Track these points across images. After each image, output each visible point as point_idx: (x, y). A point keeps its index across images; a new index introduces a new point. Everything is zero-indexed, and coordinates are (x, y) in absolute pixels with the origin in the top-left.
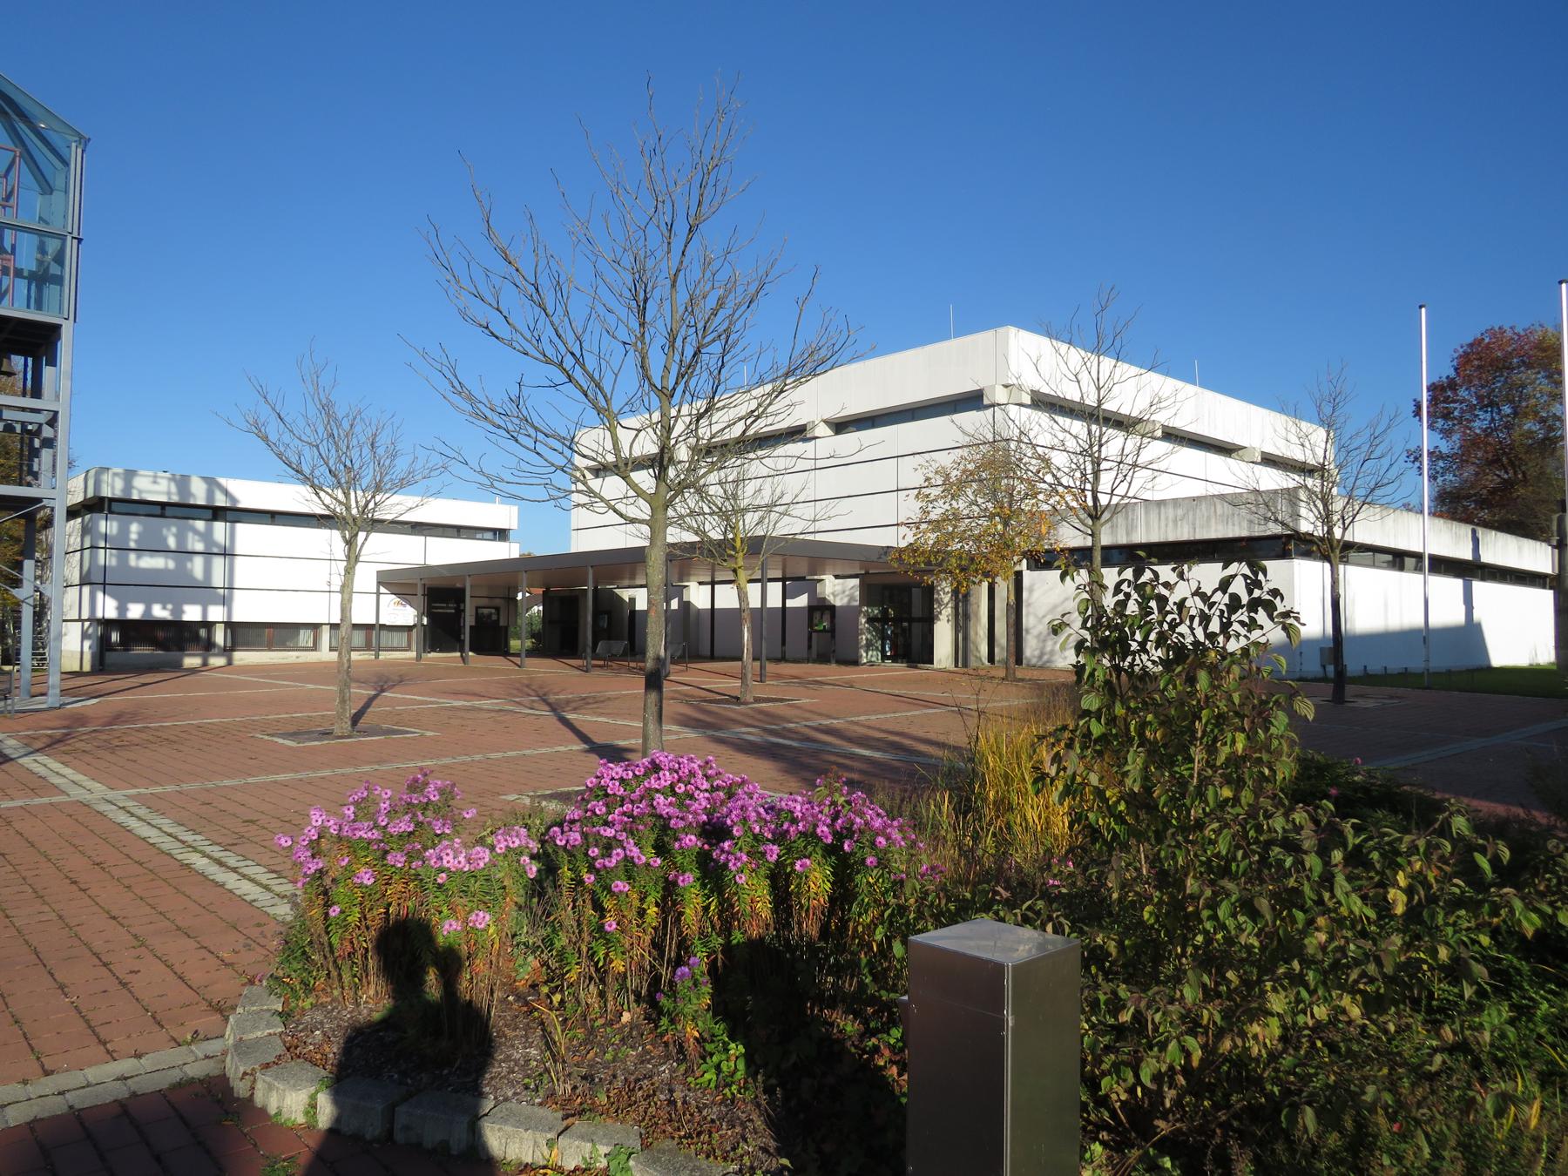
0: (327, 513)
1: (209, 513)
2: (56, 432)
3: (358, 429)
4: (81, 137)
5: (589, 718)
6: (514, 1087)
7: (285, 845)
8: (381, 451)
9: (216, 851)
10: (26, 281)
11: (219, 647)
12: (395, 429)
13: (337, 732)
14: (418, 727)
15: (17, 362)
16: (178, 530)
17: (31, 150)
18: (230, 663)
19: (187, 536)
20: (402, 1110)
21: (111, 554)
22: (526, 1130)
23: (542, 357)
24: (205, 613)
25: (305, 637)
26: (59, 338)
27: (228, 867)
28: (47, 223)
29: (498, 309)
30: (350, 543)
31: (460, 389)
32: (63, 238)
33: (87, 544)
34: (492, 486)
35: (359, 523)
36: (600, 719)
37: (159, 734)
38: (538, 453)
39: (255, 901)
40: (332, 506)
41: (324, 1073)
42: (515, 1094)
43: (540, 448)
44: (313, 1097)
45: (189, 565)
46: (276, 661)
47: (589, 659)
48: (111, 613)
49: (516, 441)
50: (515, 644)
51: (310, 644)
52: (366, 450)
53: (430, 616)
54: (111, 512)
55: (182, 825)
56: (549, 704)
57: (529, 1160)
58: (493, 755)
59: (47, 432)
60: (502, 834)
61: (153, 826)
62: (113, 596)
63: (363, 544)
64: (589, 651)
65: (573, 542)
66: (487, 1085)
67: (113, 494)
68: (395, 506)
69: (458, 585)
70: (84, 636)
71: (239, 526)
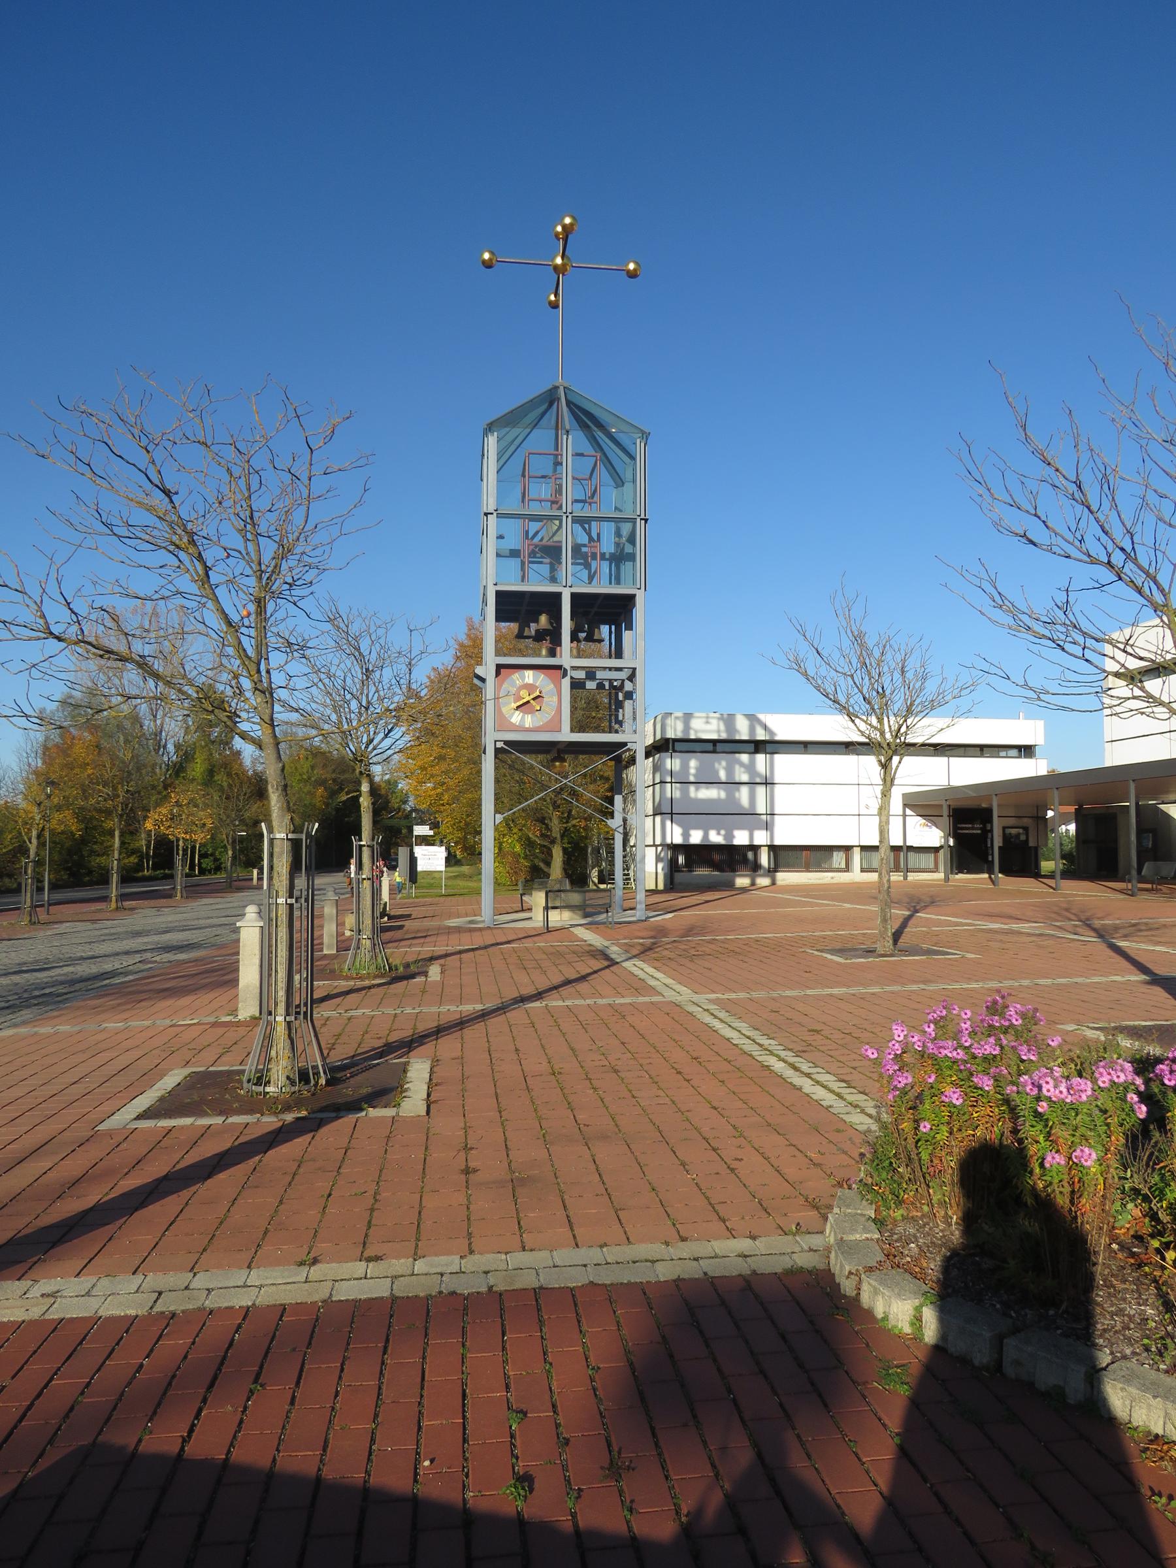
0: (863, 740)
1: (751, 747)
2: (635, 685)
3: (888, 656)
4: (643, 432)
5: (1143, 946)
6: (1132, 1345)
7: (872, 1057)
8: (910, 675)
9: (789, 1056)
10: (608, 562)
11: (764, 868)
12: (924, 651)
13: (880, 951)
14: (958, 948)
15: (605, 629)
16: (727, 764)
17: (607, 453)
18: (774, 883)
19: (734, 767)
20: (1010, 1343)
21: (676, 788)
22: (1155, 1397)
23: (1086, 558)
24: (751, 837)
25: (838, 859)
26: (634, 605)
27: (802, 1072)
28: (620, 511)
29: (1036, 515)
30: (885, 766)
31: (1001, 602)
32: (633, 521)
33: (657, 780)
34: (1039, 699)
35: (893, 747)
36: (1158, 948)
37: (726, 946)
38: (1087, 660)
39: (830, 1107)
40: (867, 732)
41: (926, 1288)
42: (1134, 1353)
43: (1089, 654)
44: (918, 1310)
45: (737, 795)
46: (811, 882)
47: (1134, 882)
48: (678, 840)
49: (1063, 649)
50: (1047, 866)
51: (843, 865)
52: (897, 675)
53: (956, 836)
54: (674, 751)
55: (757, 1029)
56: (1095, 930)
57: (1160, 1432)
58: (1042, 982)
59: (628, 686)
60: (1104, 1067)
61: (733, 1028)
62: (679, 825)
63: (898, 766)
64: (1134, 873)
65: (1107, 754)
66: (1101, 1336)
67: (676, 735)
68: (924, 730)
69: (984, 805)
70: (658, 859)
71: (776, 756)
